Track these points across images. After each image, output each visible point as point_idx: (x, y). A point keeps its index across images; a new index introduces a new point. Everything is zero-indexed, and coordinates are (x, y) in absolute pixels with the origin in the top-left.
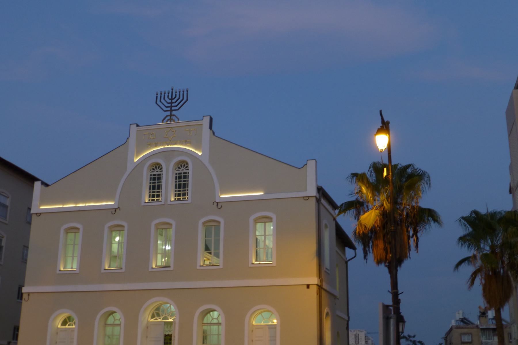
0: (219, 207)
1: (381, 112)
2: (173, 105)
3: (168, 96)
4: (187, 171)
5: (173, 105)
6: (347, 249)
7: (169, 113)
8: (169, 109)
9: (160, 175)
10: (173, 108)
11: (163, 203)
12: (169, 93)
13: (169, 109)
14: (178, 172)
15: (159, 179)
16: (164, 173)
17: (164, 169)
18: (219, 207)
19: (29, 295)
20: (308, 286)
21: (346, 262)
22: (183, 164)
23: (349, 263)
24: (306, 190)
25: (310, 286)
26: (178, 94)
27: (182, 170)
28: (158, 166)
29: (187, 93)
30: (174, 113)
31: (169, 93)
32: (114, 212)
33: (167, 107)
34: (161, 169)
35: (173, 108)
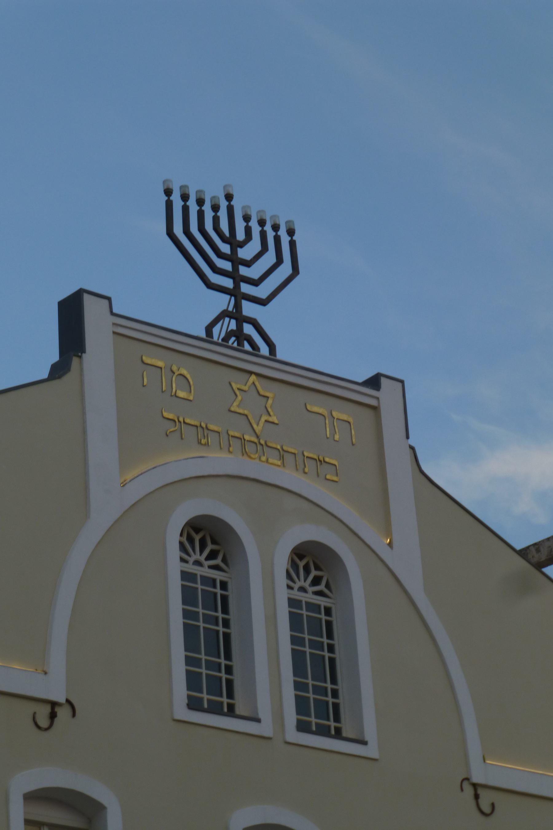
2: (243, 271)
3: (216, 220)
5: (243, 271)
8: (228, 283)
11: (265, 728)
12: (215, 208)
13: (228, 283)
26: (256, 229)
29: (293, 245)
31: (215, 208)
32: (44, 722)
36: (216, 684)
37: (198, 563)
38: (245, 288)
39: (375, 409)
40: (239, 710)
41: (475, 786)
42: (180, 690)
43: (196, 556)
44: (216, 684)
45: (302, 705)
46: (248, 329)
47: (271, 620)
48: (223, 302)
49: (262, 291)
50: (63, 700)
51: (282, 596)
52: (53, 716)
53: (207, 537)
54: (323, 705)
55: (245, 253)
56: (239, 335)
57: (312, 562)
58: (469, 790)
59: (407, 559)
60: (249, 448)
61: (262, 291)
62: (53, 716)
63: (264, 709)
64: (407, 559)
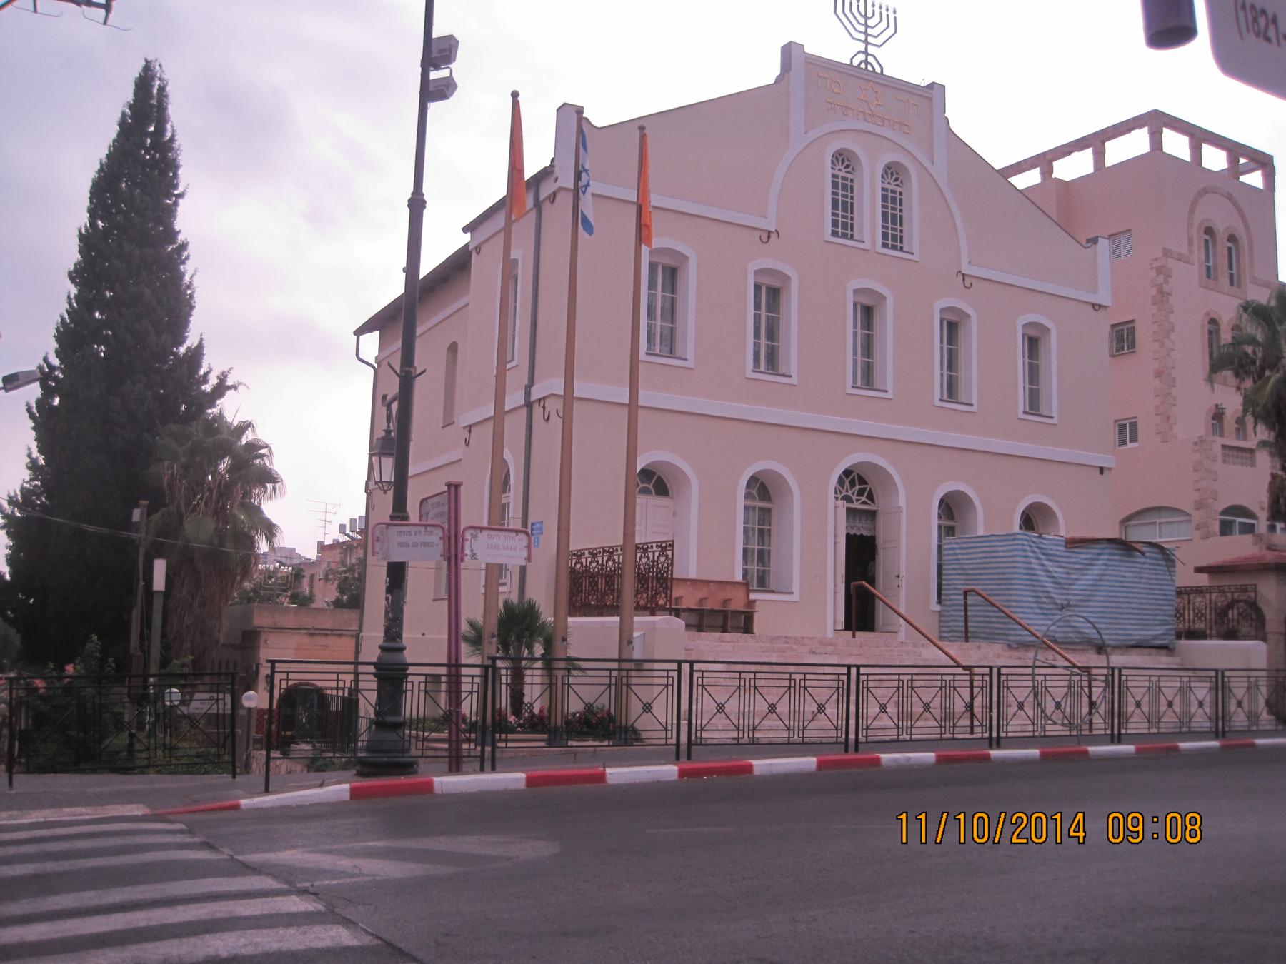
7: (862, 47)
11: (867, 246)
20: (1102, 470)
24: (1095, 292)
25: (1105, 472)
28: (843, 158)
30: (871, 49)
36: (843, 226)
38: (870, 39)
39: (930, 99)
40: (856, 237)
42: (829, 228)
44: (843, 226)
45: (885, 236)
46: (871, 59)
47: (873, 197)
48: (862, 47)
49: (878, 41)
51: (879, 186)
53: (843, 158)
54: (893, 237)
55: (870, 23)
56: (866, 62)
57: (893, 171)
58: (960, 277)
60: (868, 117)
61: (878, 41)
63: (867, 238)
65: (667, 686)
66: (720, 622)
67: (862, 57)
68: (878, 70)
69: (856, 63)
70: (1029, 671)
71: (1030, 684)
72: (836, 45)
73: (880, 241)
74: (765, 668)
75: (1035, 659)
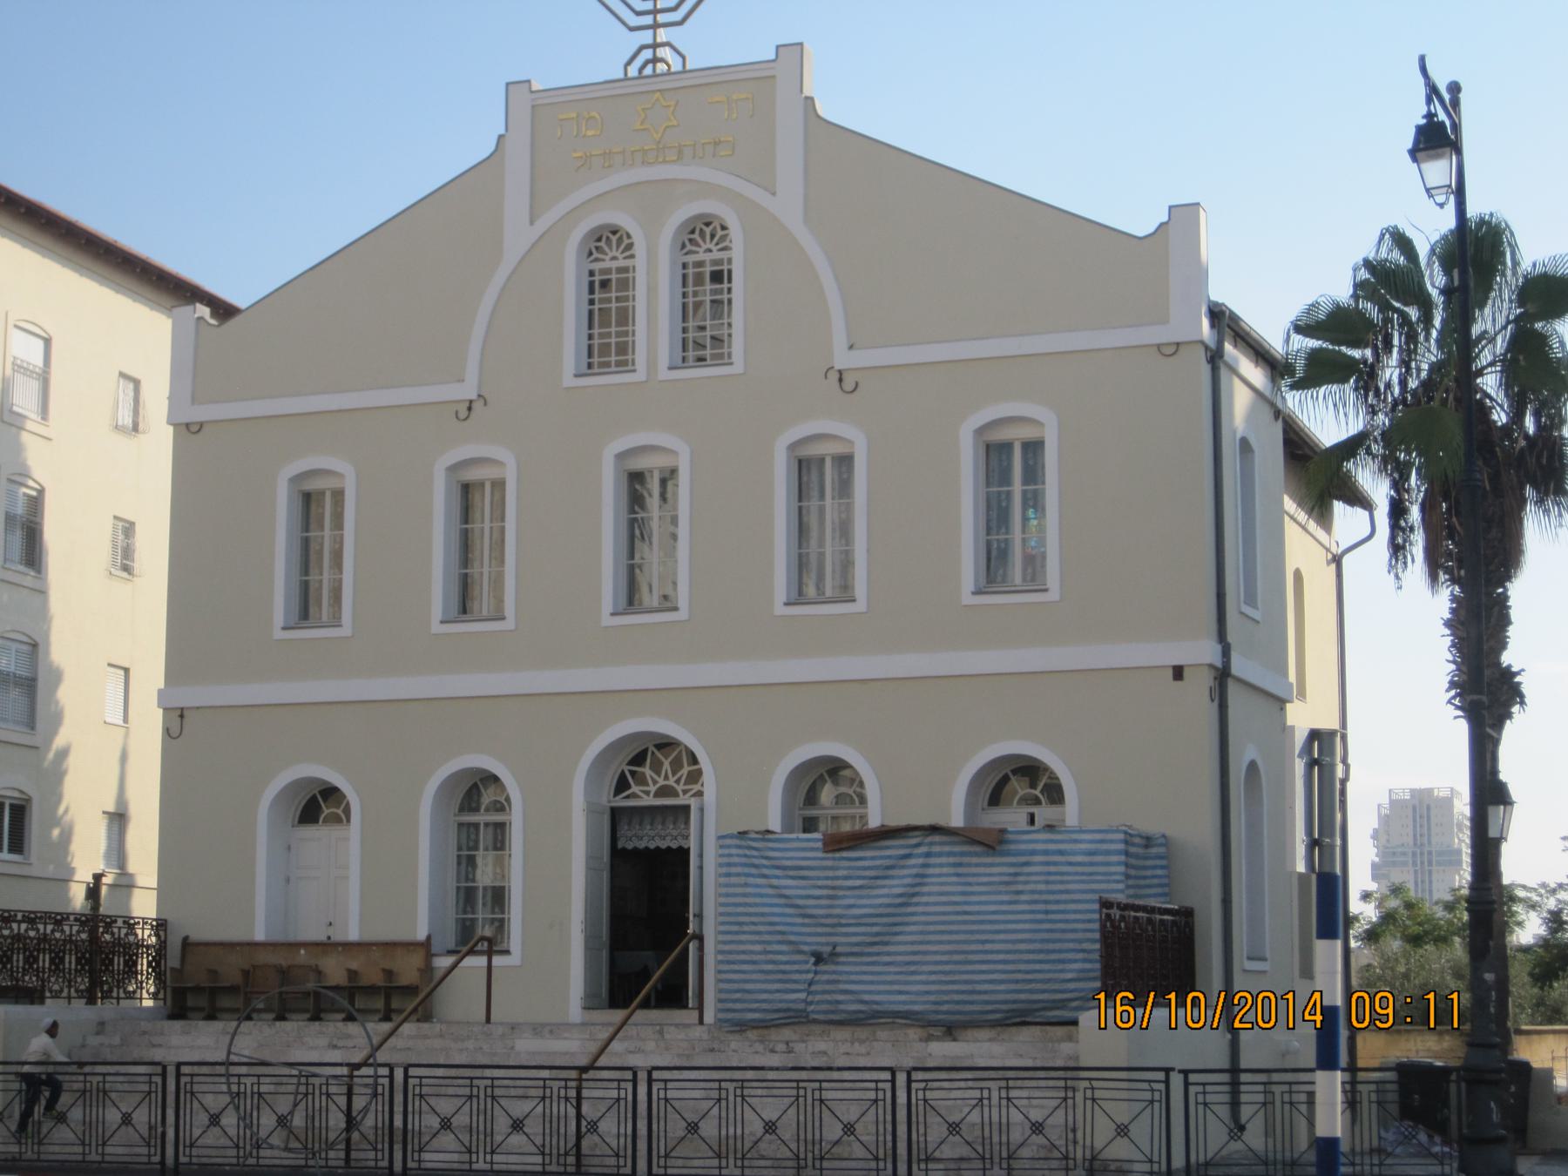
0: (848, 386)
1: (1422, 59)
4: (724, 255)
6: (1339, 507)
7: (646, 37)
8: (648, 20)
9: (625, 270)
10: (661, 18)
13: (648, 20)
14: (691, 259)
15: (625, 284)
16: (640, 262)
17: (640, 249)
18: (848, 386)
19: (182, 716)
20: (1178, 672)
21: (1337, 560)
22: (703, 229)
23: (1346, 560)
24: (1164, 321)
25: (1186, 673)
27: (706, 254)
33: (638, 14)
34: (630, 246)
35: (661, 18)
37: (614, 258)
41: (840, 372)
43: (614, 253)
46: (661, 52)
47: (652, 289)
50: (473, 396)
52: (470, 409)
56: (655, 60)
58: (834, 376)
59: (787, 204)
62: (470, 409)
64: (787, 205)
65: (719, 1100)
66: (380, 1004)
67: (647, 54)
68: (676, 65)
69: (633, 71)
70: (221, 1070)
71: (224, 1088)
72: (598, 54)
73: (663, 359)
74: (205, 1070)
75: (229, 1053)
